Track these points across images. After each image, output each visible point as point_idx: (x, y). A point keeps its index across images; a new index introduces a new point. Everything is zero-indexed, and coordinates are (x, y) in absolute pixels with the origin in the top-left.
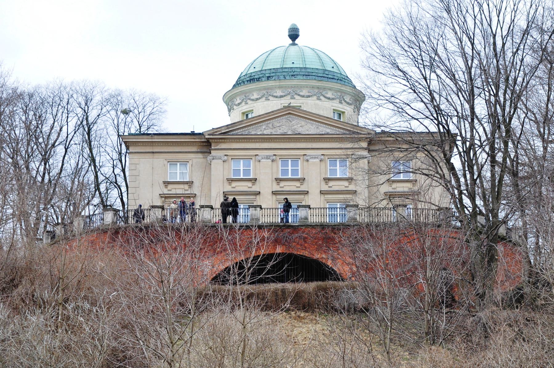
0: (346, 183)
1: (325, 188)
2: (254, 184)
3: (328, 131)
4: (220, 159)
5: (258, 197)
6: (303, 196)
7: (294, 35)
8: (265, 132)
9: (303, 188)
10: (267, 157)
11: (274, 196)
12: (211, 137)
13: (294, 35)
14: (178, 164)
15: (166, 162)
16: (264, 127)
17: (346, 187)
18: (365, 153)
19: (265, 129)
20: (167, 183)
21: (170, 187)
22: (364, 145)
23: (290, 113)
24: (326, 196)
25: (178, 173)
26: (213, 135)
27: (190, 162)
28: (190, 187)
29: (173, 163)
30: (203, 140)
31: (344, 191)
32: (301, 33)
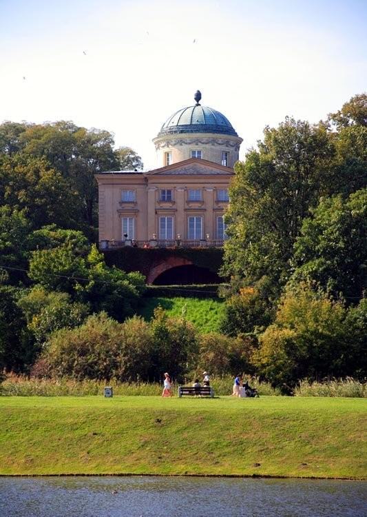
7: (198, 97)
9: (203, 207)
10: (181, 188)
13: (198, 97)
20: (122, 203)
21: (123, 205)
25: (129, 196)
28: (135, 205)
32: (202, 96)
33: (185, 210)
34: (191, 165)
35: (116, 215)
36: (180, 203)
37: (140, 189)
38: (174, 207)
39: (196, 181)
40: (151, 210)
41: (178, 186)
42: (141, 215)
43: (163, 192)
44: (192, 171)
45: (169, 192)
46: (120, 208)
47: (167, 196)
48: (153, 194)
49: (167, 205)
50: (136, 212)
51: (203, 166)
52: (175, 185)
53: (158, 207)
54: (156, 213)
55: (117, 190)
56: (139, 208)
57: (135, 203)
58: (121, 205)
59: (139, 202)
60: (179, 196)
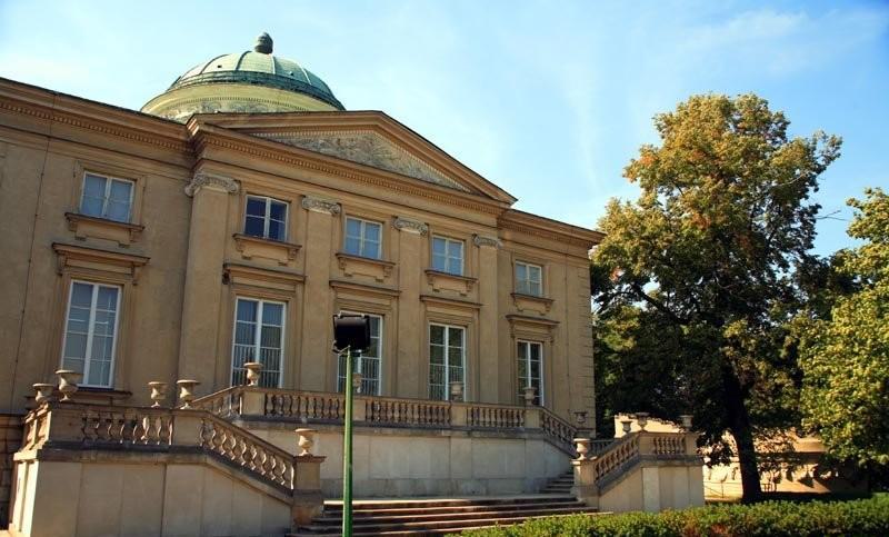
0: (462, 288)
1: (428, 290)
2: (292, 258)
3: (438, 180)
4: (225, 184)
5: (299, 289)
6: (387, 303)
7: (266, 46)
8: (323, 150)
9: (389, 283)
10: (325, 205)
11: (333, 293)
12: (211, 130)
13: (266, 46)
14: (110, 179)
15: (78, 169)
16: (321, 142)
17: (462, 295)
18: (492, 235)
19: (323, 145)
20: (73, 219)
21: (83, 229)
22: (492, 221)
23: (376, 128)
24: (429, 309)
25: (109, 198)
26: (216, 126)
27: (142, 182)
29: (97, 173)
30: (182, 138)
31: (459, 301)
33: (332, 284)
34: (359, 135)
35: (46, 265)
36: (318, 261)
37: (160, 181)
38: (294, 267)
39: (372, 191)
40: (205, 261)
41: (314, 195)
42: (154, 282)
43: (256, 207)
44: (359, 155)
45: (278, 210)
46: (69, 238)
47: (263, 222)
48: (216, 204)
49: (268, 256)
50: (137, 265)
51: (394, 150)
52: (305, 189)
53: (236, 257)
54: (226, 278)
55: (61, 164)
56: (148, 247)
57: (135, 230)
58: (72, 228)
59: (152, 232)
60: (315, 228)
